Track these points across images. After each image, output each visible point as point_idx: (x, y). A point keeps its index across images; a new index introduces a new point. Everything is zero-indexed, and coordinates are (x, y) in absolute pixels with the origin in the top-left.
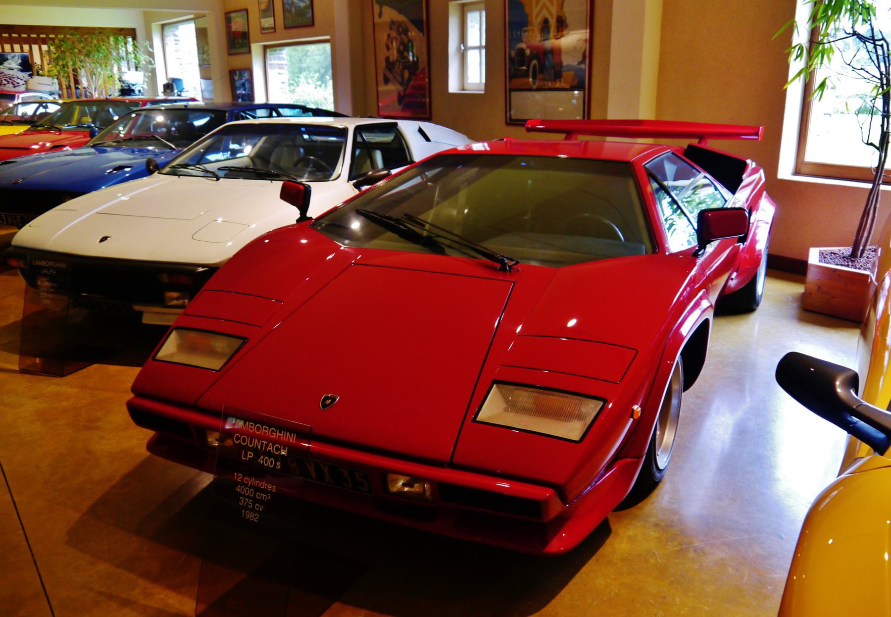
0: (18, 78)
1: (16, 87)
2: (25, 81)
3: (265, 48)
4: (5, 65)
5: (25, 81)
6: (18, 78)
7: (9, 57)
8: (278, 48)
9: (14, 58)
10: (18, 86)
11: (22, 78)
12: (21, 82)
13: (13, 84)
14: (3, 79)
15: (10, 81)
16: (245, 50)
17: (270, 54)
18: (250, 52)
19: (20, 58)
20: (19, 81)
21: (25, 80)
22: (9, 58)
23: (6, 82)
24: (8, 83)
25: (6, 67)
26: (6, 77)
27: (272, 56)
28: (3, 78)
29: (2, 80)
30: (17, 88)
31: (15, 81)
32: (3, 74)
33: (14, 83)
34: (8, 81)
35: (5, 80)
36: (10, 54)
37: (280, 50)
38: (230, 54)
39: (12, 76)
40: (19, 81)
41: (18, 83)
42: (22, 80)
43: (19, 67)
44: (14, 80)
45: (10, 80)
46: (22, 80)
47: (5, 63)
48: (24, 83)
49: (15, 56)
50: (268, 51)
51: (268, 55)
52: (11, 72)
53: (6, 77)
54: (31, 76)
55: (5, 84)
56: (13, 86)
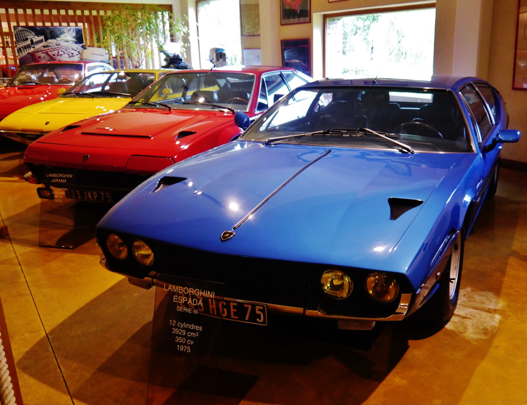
0: (73, 49)
1: (71, 57)
2: (79, 52)
3: (325, 17)
4: (62, 38)
5: (79, 52)
6: (73, 49)
7: (65, 30)
8: (336, 18)
9: (70, 32)
10: (72, 56)
11: (76, 49)
12: (75, 53)
13: (69, 55)
15: (66, 52)
16: (307, 19)
17: (329, 24)
18: (310, 21)
19: (75, 32)
20: (73, 52)
21: (78, 51)
22: (65, 32)
23: (62, 53)
24: (64, 54)
25: (62, 39)
26: (63, 48)
27: (330, 26)
28: (60, 49)
29: (59, 51)
30: (72, 57)
31: (70, 52)
32: (60, 46)
33: (70, 54)
34: (64, 52)
35: (62, 51)
36: (66, 28)
37: (338, 20)
38: (282, 25)
39: (68, 47)
40: (73, 52)
41: (72, 54)
42: (76, 51)
43: (74, 39)
44: (70, 50)
45: (66, 51)
46: (76, 51)
47: (62, 36)
48: (78, 53)
49: (70, 30)
50: (328, 20)
51: (327, 25)
52: (66, 44)
53: (63, 48)
54: (84, 47)
55: (61, 55)
56: (68, 56)
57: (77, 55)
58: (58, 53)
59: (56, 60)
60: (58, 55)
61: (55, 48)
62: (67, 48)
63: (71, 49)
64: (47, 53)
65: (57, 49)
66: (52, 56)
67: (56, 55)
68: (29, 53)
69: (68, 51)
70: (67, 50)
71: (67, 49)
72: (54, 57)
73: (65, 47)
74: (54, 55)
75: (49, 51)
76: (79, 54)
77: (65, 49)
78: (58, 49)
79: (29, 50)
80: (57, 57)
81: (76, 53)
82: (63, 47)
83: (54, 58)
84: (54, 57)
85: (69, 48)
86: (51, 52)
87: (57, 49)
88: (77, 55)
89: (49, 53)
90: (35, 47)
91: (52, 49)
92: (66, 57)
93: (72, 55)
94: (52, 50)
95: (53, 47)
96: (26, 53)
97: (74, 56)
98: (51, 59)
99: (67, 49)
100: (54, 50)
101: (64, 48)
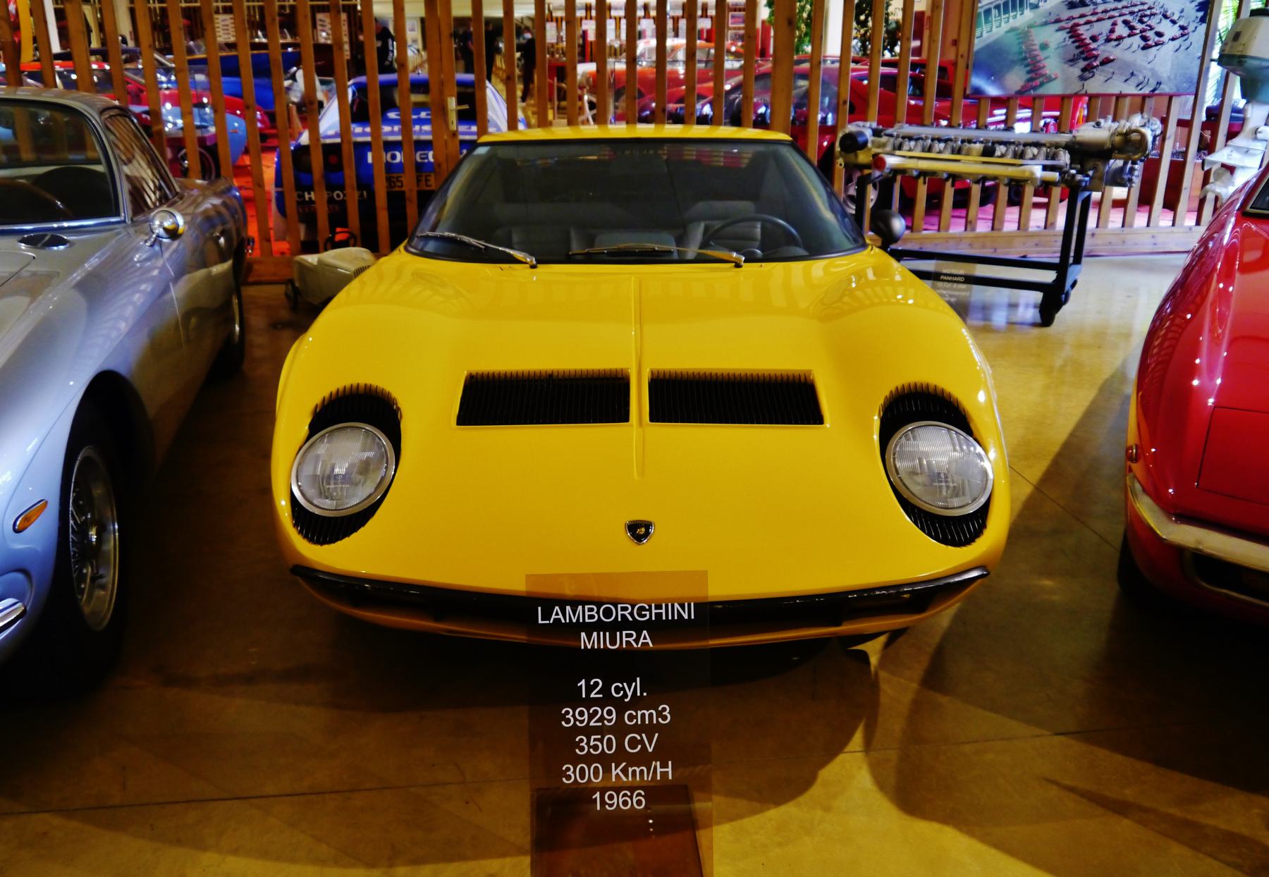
0: (1165, 16)
2: (1182, 28)
5: (1182, 28)
6: (1165, 16)
10: (1157, 44)
11: (1175, 18)
12: (1169, 30)
13: (1145, 39)
14: (1120, 20)
15: (1140, 26)
21: (1181, 23)
24: (1129, 36)
29: (1114, 24)
31: (1152, 28)
33: (1150, 34)
34: (1132, 28)
41: (1159, 34)
42: (1174, 22)
44: (1153, 22)
45: (1141, 21)
53: (1132, 13)
55: (1120, 38)
56: (1142, 43)
57: (1173, 39)
58: (1112, 31)
59: (1096, 57)
60: (1108, 40)
61: (1105, 11)
62: (1148, 12)
63: (1160, 16)
64: (1073, 33)
65: (1112, 13)
66: (1088, 41)
67: (1102, 39)
68: (1012, 30)
69: (1148, 23)
70: (1145, 19)
71: (1145, 16)
72: (1093, 46)
73: (1141, 7)
74: (1094, 39)
75: (1082, 21)
76: (1183, 35)
77: (1139, 14)
78: (1116, 13)
79: (1015, 17)
80: (1102, 48)
81: (1175, 31)
82: (1136, 5)
83: (1094, 49)
84: (1093, 46)
85: (1154, 11)
86: (1087, 27)
87: (1112, 13)
88: (1173, 39)
89: (1081, 30)
90: (1041, 4)
91: (1094, 14)
92: (1135, 47)
93: (1157, 39)
94: (1094, 18)
95: (1100, 8)
96: (1005, 27)
97: (1163, 44)
98: (1082, 53)
99: (1145, 16)
100: (1098, 20)
101: (1136, 9)
